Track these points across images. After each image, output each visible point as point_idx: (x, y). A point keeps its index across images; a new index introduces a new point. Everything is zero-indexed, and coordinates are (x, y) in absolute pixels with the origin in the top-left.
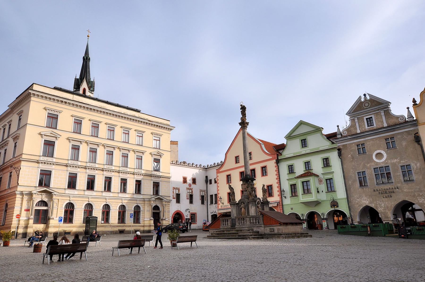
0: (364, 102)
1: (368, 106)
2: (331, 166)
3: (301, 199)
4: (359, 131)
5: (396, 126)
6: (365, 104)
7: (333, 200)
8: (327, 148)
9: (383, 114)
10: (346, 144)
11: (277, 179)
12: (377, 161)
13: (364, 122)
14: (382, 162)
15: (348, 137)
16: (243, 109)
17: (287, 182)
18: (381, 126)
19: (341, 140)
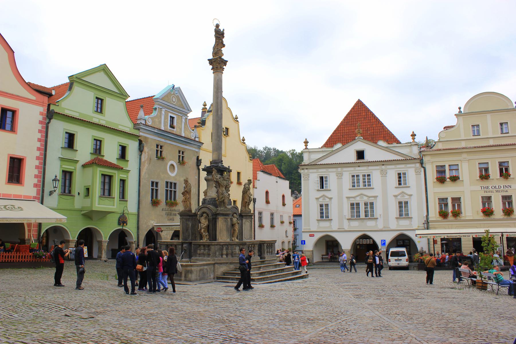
1: (174, 102)
2: (128, 161)
3: (97, 205)
4: (163, 128)
5: (191, 141)
6: (172, 98)
7: (123, 214)
8: (127, 130)
9: (184, 120)
10: (148, 138)
11: (39, 149)
13: (168, 118)
14: (173, 177)
15: (155, 130)
16: (219, 35)
17: (58, 163)
18: (178, 134)
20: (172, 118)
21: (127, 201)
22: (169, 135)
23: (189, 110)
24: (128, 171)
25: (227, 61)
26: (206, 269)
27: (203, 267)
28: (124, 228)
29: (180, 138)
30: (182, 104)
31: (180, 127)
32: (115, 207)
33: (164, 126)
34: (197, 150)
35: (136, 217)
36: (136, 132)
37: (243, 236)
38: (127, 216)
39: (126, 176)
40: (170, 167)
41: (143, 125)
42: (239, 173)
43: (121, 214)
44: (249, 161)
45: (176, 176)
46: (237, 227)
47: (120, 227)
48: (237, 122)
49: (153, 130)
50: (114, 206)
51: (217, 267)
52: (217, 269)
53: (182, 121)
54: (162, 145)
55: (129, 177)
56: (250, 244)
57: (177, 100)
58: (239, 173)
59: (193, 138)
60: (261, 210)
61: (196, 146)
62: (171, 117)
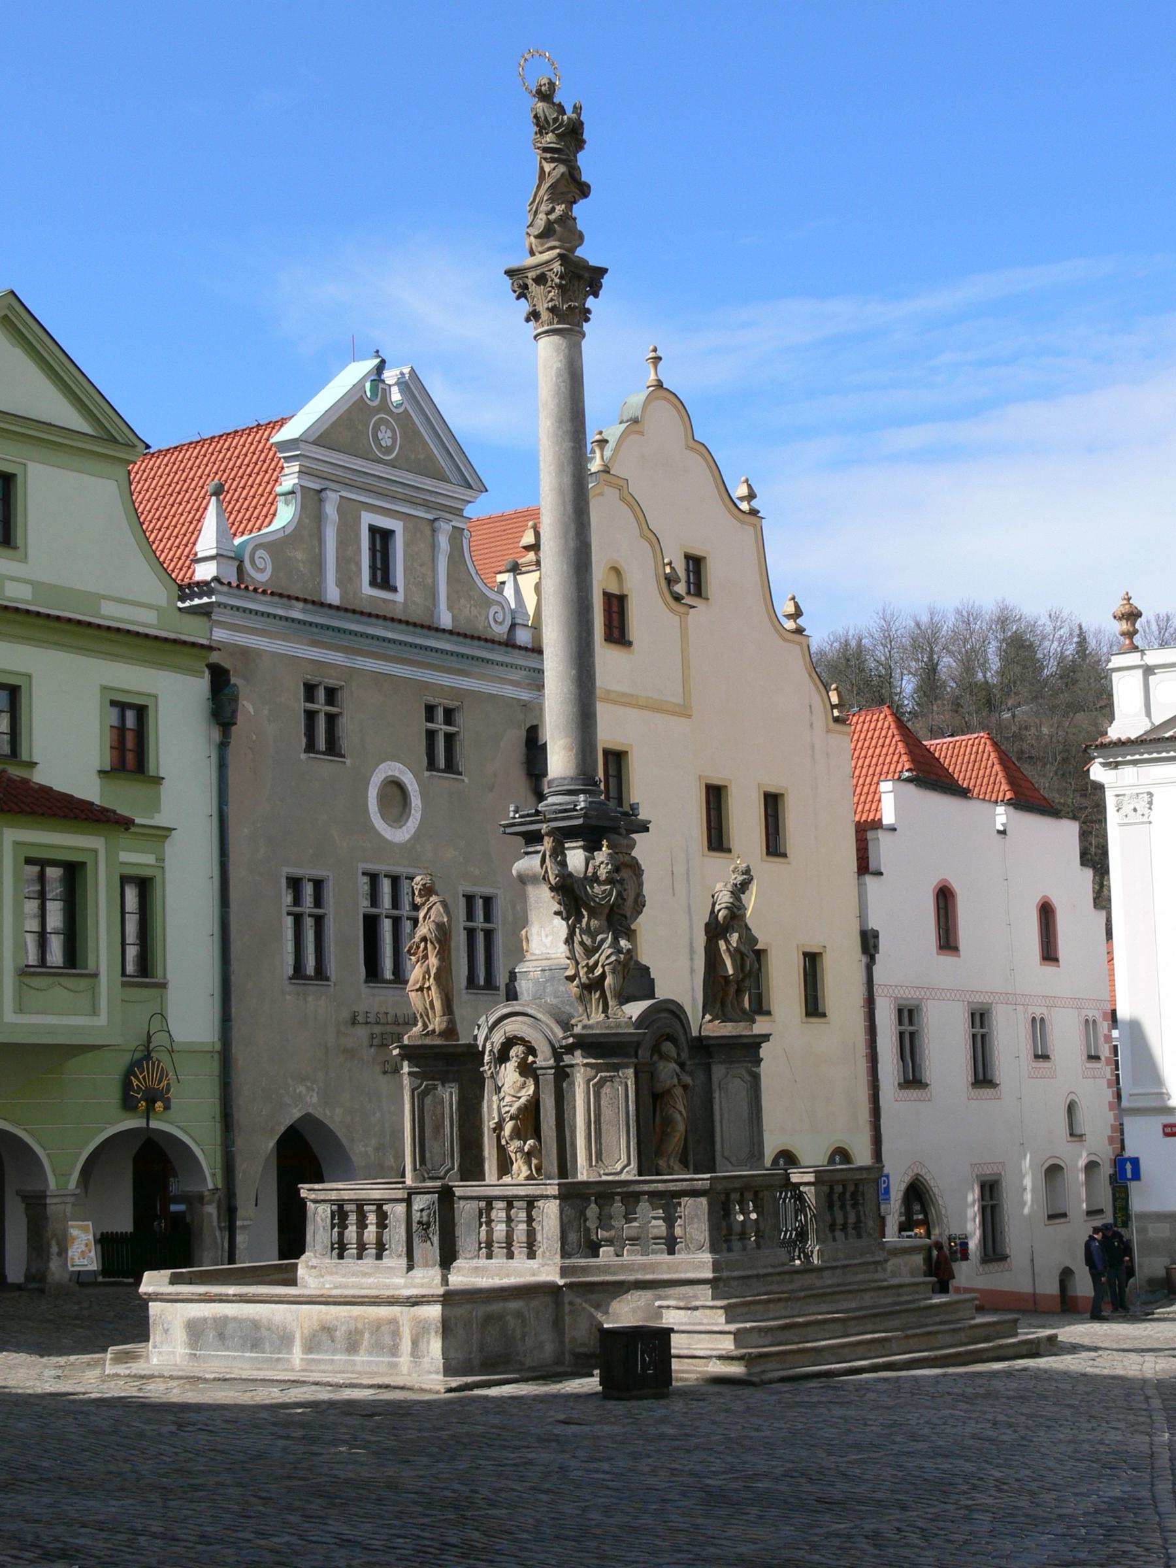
0: (391, 413)
1: (389, 451)
4: (333, 595)
6: (376, 429)
8: (145, 620)
9: (443, 541)
10: (259, 653)
12: (383, 833)
14: (401, 846)
15: (291, 607)
19: (245, 610)
20: (382, 538)
21: (163, 986)
22: (371, 631)
23: (470, 487)
24: (163, 834)
25: (604, 271)
26: (519, 1314)
27: (501, 1304)
28: (154, 1124)
29: (427, 637)
30: (430, 457)
31: (429, 580)
32: (102, 1020)
33: (340, 583)
34: (524, 695)
35: (214, 1066)
36: (194, 630)
37: (718, 1146)
38: (165, 1059)
39: (150, 859)
40: (382, 799)
41: (225, 589)
42: (773, 803)
43: (138, 1056)
44: (832, 725)
45: (417, 837)
46: (679, 1111)
47: (133, 1123)
48: (752, 519)
49: (281, 612)
50: (95, 1012)
51: (571, 1303)
52: (571, 1312)
53: (434, 546)
54: (332, 682)
55: (168, 864)
56: (734, 1190)
57: (404, 435)
58: (773, 803)
59: (500, 631)
60: (909, 995)
61: (516, 676)
62: (373, 530)
